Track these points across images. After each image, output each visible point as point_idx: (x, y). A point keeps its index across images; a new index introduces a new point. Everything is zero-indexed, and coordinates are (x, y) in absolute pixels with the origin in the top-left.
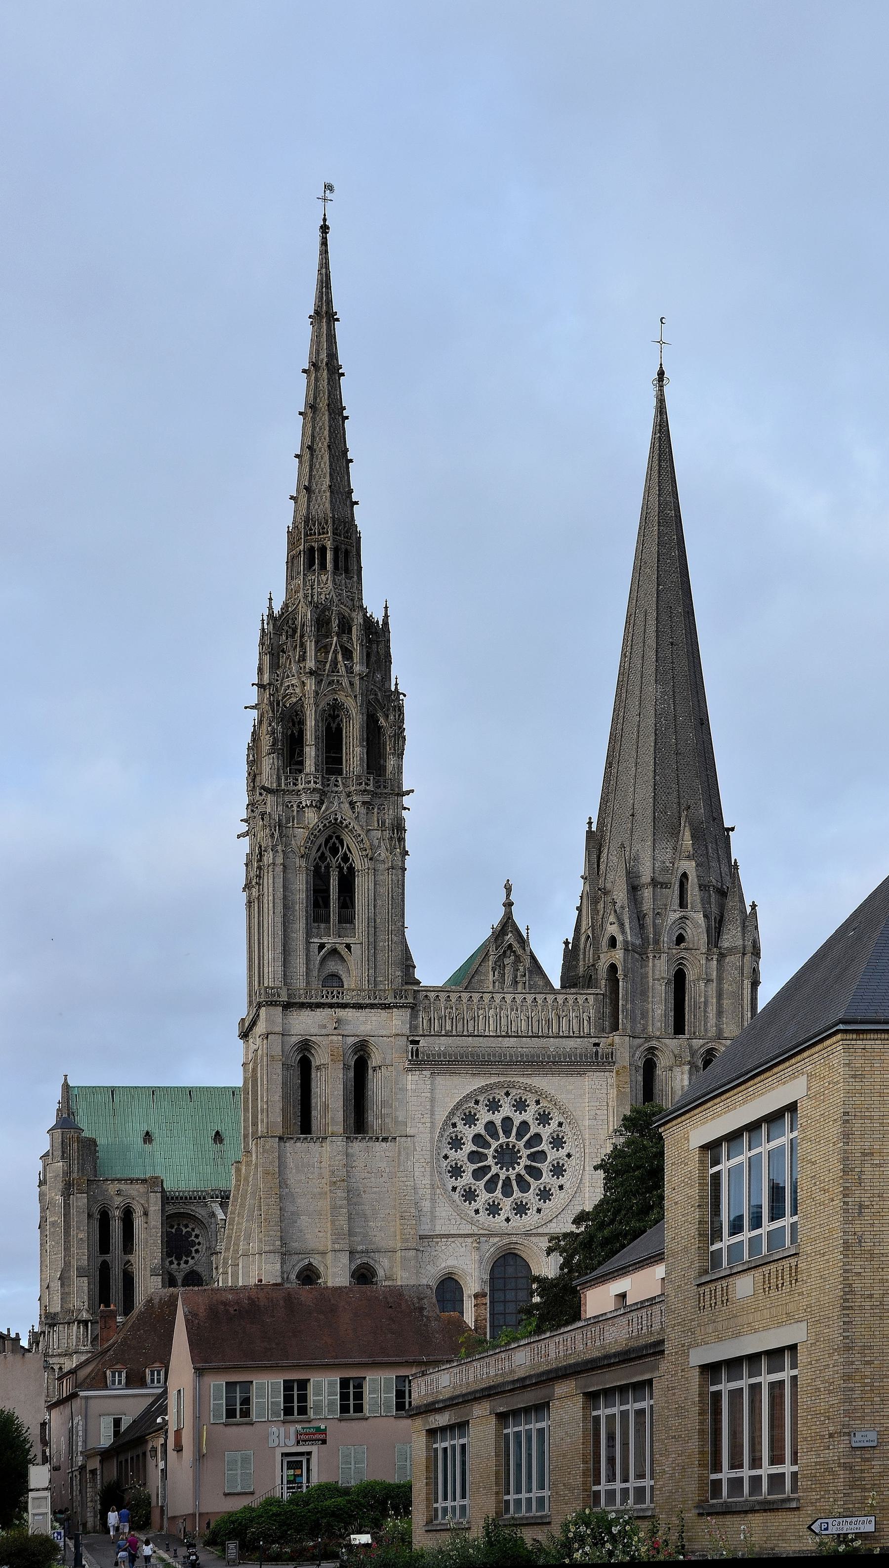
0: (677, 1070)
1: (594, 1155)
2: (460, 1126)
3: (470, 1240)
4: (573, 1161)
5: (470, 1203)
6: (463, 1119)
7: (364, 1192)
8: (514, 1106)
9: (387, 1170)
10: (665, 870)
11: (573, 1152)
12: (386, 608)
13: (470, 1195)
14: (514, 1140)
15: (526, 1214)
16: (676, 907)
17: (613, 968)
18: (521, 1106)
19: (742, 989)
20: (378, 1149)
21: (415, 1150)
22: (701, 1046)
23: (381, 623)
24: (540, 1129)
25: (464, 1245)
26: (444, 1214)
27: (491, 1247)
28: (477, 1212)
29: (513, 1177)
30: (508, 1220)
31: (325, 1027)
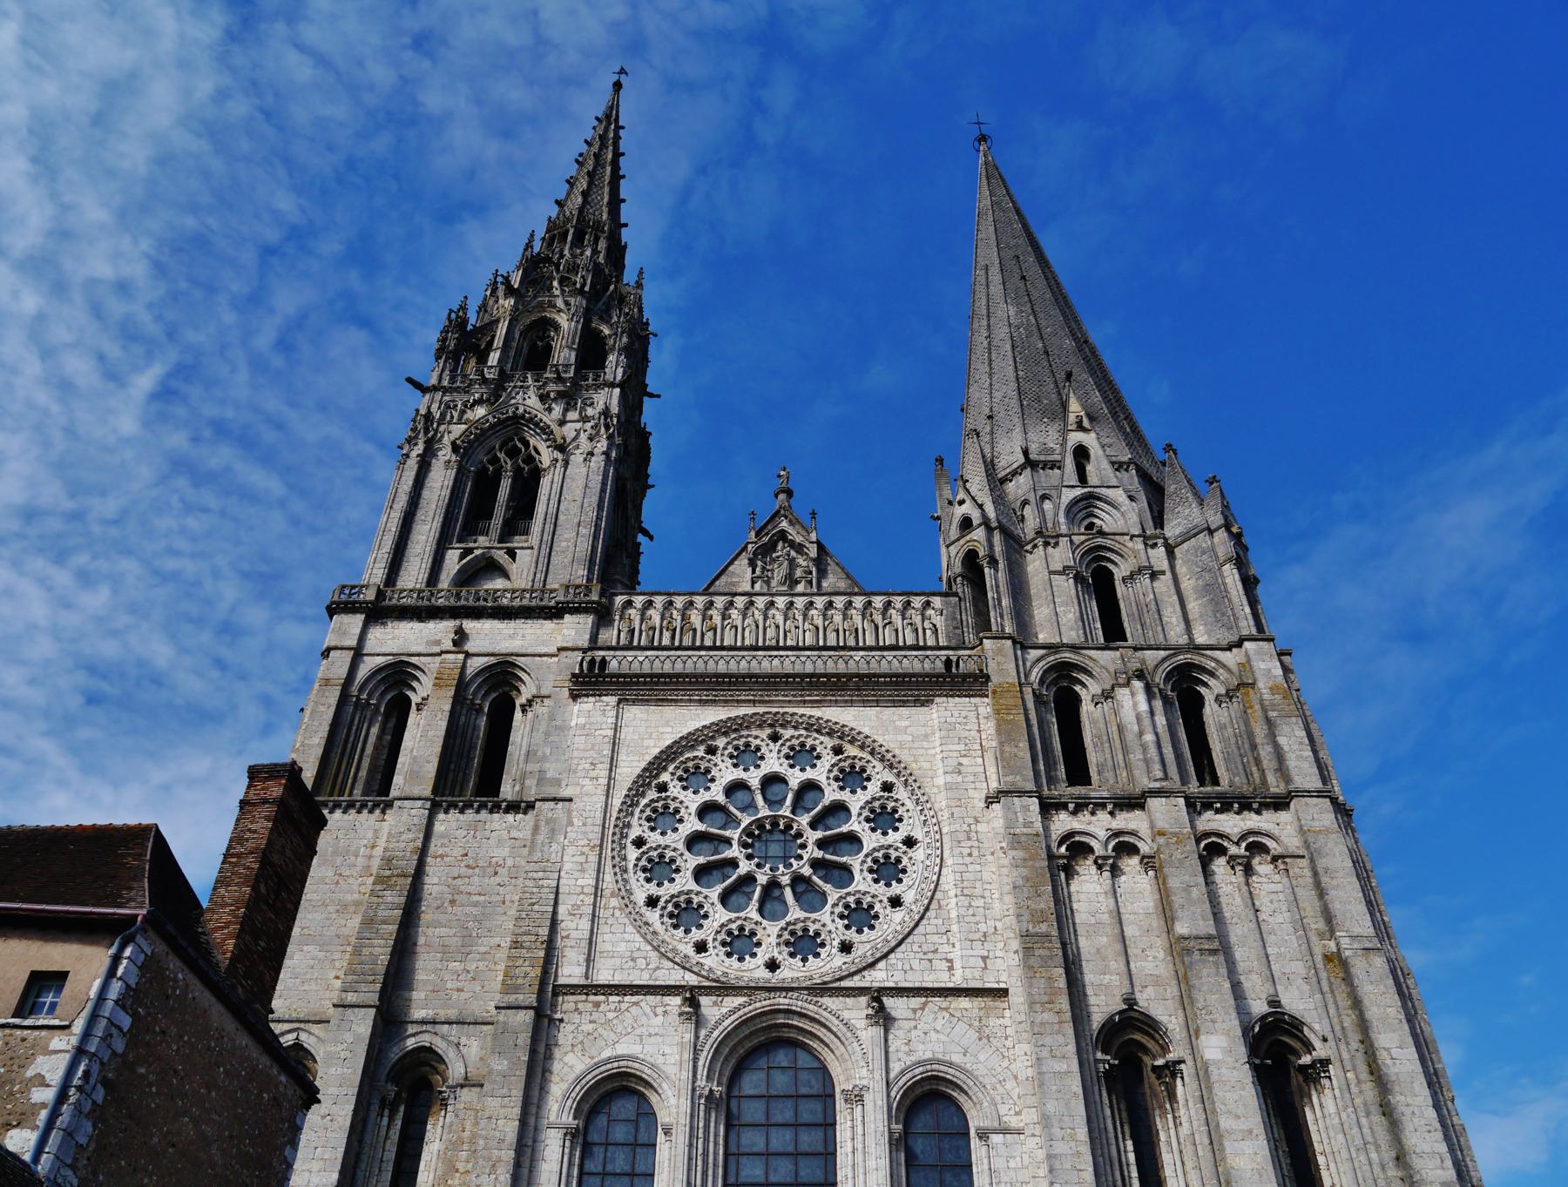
0: (1122, 694)
1: (962, 836)
2: (675, 789)
3: (677, 1000)
4: (919, 853)
5: (687, 931)
6: (680, 779)
7: (453, 902)
8: (787, 757)
9: (509, 862)
10: (1048, 451)
11: (918, 834)
12: (641, 273)
13: (685, 913)
14: (788, 814)
15: (817, 955)
16: (1074, 480)
17: (971, 557)
18: (801, 755)
19: (1223, 577)
20: (496, 825)
21: (570, 823)
22: (1164, 659)
23: (632, 283)
24: (845, 796)
25: (660, 1010)
26: (622, 947)
27: (720, 1012)
28: (701, 947)
29: (785, 880)
30: (772, 965)
31: (438, 643)
